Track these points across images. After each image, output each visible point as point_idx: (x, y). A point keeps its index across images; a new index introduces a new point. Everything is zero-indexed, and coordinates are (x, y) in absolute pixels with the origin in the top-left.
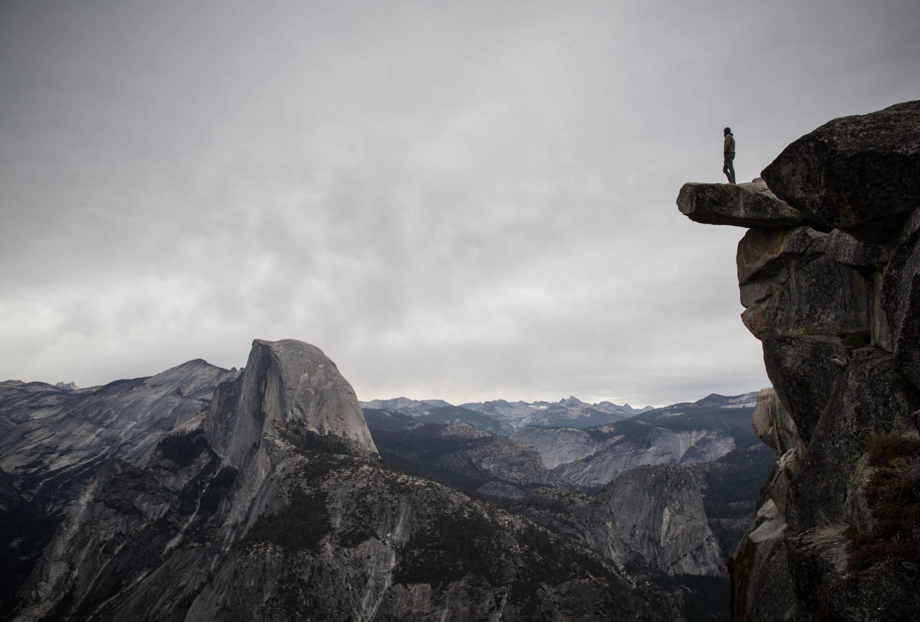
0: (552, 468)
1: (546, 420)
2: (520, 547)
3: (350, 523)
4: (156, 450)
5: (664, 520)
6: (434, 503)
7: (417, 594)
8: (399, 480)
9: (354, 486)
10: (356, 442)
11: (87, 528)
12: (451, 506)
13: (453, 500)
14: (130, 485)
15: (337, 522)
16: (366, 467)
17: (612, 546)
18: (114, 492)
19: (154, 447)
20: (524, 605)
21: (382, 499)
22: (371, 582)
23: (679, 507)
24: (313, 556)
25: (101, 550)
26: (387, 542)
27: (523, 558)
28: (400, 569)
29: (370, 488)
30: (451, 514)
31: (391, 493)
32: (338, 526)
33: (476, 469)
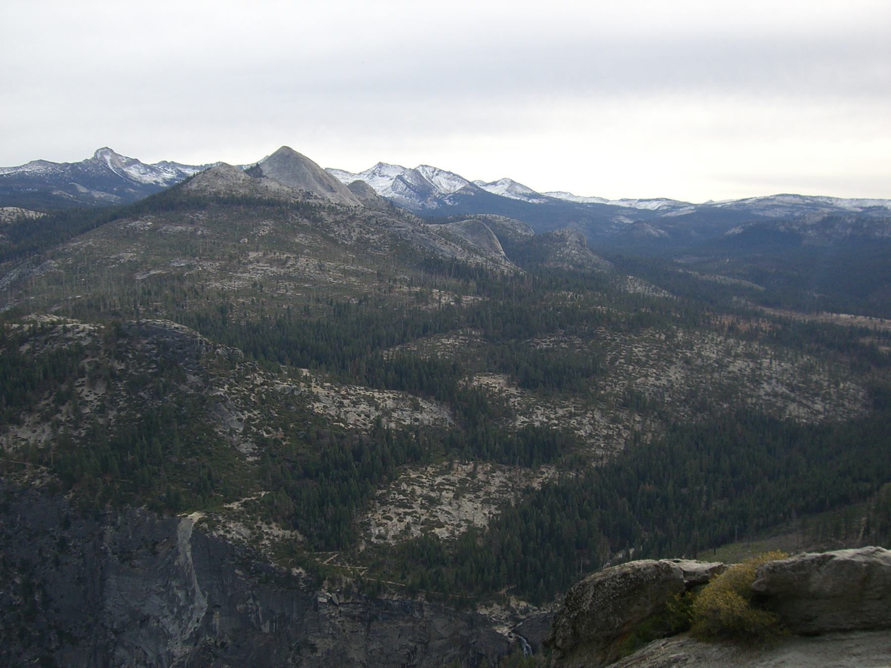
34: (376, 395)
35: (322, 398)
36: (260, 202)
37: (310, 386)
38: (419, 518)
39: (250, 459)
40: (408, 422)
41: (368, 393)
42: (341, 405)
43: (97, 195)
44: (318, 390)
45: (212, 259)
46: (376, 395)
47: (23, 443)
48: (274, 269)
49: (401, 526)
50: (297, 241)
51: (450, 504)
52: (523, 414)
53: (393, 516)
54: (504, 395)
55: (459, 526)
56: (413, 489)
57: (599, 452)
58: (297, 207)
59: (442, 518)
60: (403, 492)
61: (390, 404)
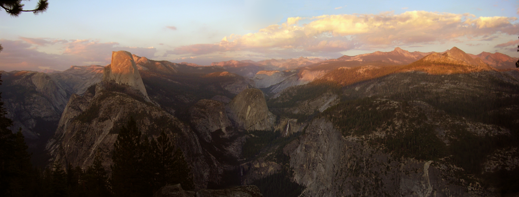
0: (268, 87)
1: (288, 67)
2: (150, 123)
3: (104, 114)
4: (87, 90)
5: (248, 110)
6: (131, 108)
7: (113, 137)
8: (125, 100)
9: (110, 103)
10: (130, 86)
11: (67, 114)
12: (136, 109)
13: (139, 107)
14: (78, 101)
15: (101, 114)
16: (118, 96)
17: (221, 121)
18: (74, 104)
19: (87, 89)
20: (143, 142)
21: (116, 107)
22: (103, 133)
23: (255, 105)
24: (89, 124)
25: (70, 121)
26: (113, 121)
27: (149, 126)
28: (112, 129)
29: (114, 103)
30: (135, 112)
31: (120, 104)
32: (100, 115)
34: (486, 126)
35: (470, 126)
36: (447, 64)
37: (466, 123)
38: (501, 164)
39: (447, 145)
41: (484, 125)
42: (476, 129)
43: (395, 61)
44: (468, 124)
45: (433, 82)
46: (486, 126)
47: (377, 137)
49: (495, 166)
50: (460, 77)
51: (510, 160)
53: (492, 163)
56: (499, 155)
58: (459, 66)
59: (508, 164)
60: (495, 156)
61: (491, 128)
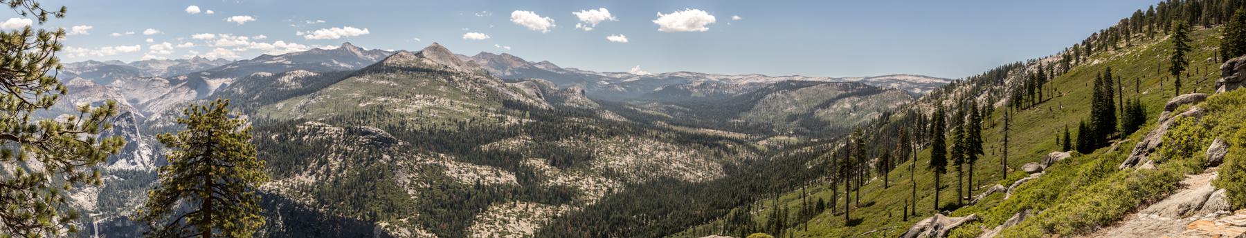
33: (72, 107)
34: (478, 168)
36: (423, 70)
37: (444, 163)
39: (413, 197)
40: (493, 182)
42: (460, 172)
43: (342, 65)
44: (450, 166)
45: (397, 97)
46: (478, 168)
47: (302, 183)
48: (428, 104)
50: (440, 89)
52: (552, 179)
54: (542, 169)
55: (519, 234)
57: (591, 198)
58: (440, 72)
61: (485, 173)
